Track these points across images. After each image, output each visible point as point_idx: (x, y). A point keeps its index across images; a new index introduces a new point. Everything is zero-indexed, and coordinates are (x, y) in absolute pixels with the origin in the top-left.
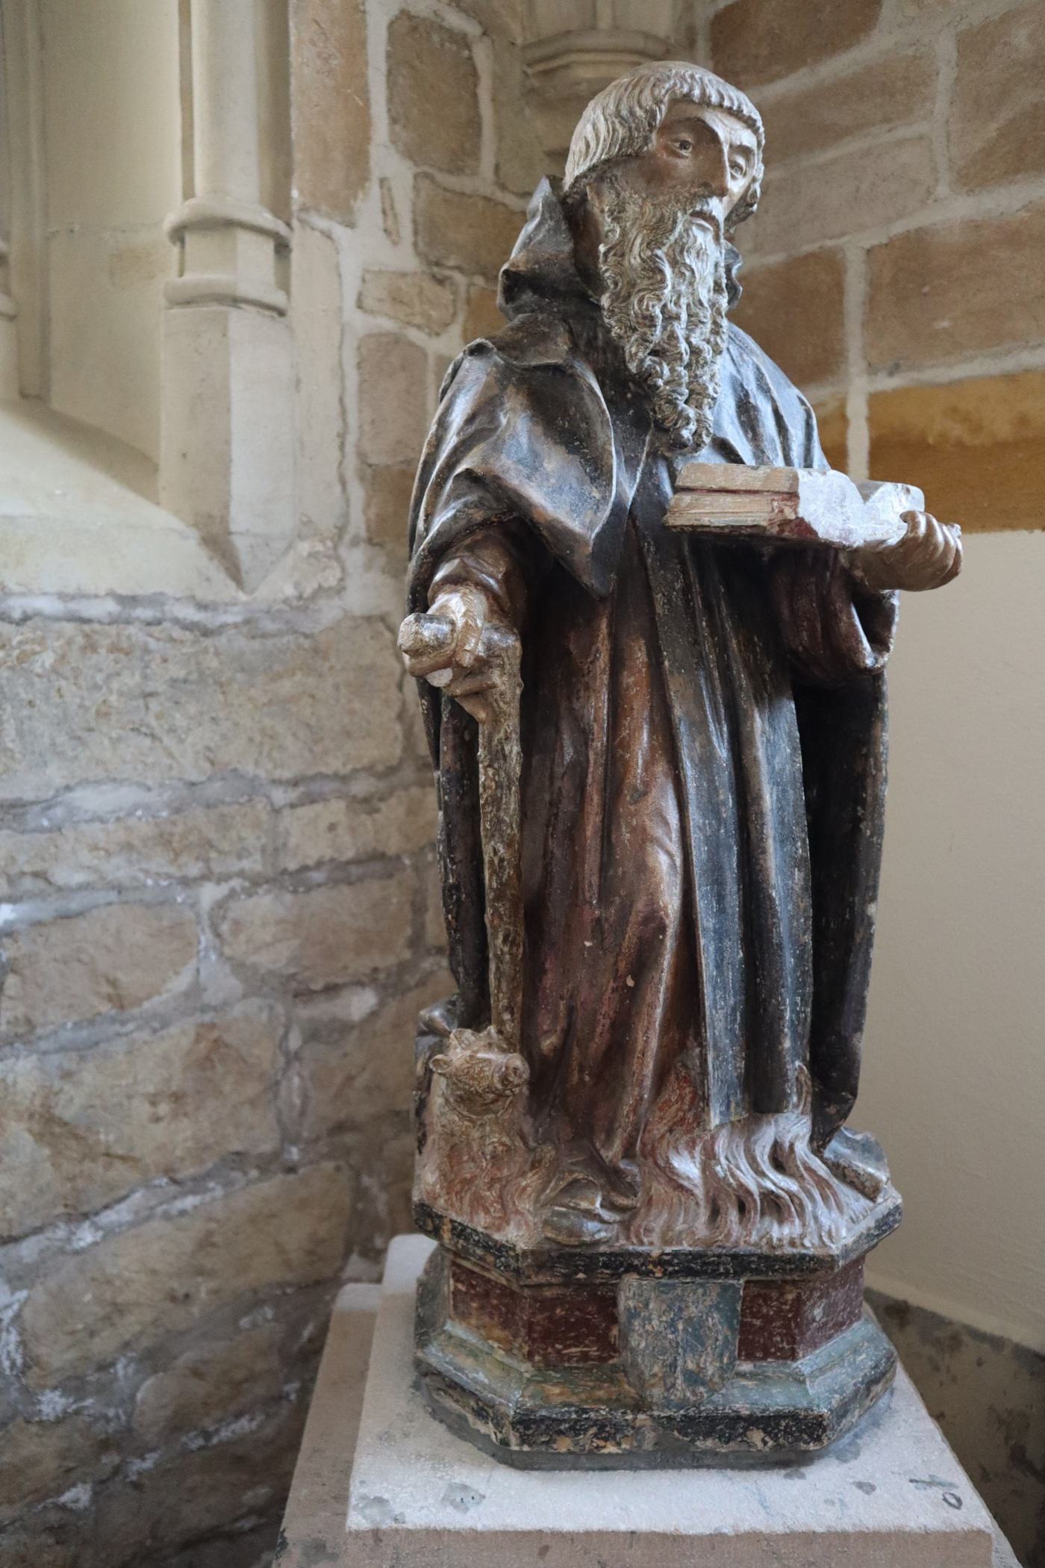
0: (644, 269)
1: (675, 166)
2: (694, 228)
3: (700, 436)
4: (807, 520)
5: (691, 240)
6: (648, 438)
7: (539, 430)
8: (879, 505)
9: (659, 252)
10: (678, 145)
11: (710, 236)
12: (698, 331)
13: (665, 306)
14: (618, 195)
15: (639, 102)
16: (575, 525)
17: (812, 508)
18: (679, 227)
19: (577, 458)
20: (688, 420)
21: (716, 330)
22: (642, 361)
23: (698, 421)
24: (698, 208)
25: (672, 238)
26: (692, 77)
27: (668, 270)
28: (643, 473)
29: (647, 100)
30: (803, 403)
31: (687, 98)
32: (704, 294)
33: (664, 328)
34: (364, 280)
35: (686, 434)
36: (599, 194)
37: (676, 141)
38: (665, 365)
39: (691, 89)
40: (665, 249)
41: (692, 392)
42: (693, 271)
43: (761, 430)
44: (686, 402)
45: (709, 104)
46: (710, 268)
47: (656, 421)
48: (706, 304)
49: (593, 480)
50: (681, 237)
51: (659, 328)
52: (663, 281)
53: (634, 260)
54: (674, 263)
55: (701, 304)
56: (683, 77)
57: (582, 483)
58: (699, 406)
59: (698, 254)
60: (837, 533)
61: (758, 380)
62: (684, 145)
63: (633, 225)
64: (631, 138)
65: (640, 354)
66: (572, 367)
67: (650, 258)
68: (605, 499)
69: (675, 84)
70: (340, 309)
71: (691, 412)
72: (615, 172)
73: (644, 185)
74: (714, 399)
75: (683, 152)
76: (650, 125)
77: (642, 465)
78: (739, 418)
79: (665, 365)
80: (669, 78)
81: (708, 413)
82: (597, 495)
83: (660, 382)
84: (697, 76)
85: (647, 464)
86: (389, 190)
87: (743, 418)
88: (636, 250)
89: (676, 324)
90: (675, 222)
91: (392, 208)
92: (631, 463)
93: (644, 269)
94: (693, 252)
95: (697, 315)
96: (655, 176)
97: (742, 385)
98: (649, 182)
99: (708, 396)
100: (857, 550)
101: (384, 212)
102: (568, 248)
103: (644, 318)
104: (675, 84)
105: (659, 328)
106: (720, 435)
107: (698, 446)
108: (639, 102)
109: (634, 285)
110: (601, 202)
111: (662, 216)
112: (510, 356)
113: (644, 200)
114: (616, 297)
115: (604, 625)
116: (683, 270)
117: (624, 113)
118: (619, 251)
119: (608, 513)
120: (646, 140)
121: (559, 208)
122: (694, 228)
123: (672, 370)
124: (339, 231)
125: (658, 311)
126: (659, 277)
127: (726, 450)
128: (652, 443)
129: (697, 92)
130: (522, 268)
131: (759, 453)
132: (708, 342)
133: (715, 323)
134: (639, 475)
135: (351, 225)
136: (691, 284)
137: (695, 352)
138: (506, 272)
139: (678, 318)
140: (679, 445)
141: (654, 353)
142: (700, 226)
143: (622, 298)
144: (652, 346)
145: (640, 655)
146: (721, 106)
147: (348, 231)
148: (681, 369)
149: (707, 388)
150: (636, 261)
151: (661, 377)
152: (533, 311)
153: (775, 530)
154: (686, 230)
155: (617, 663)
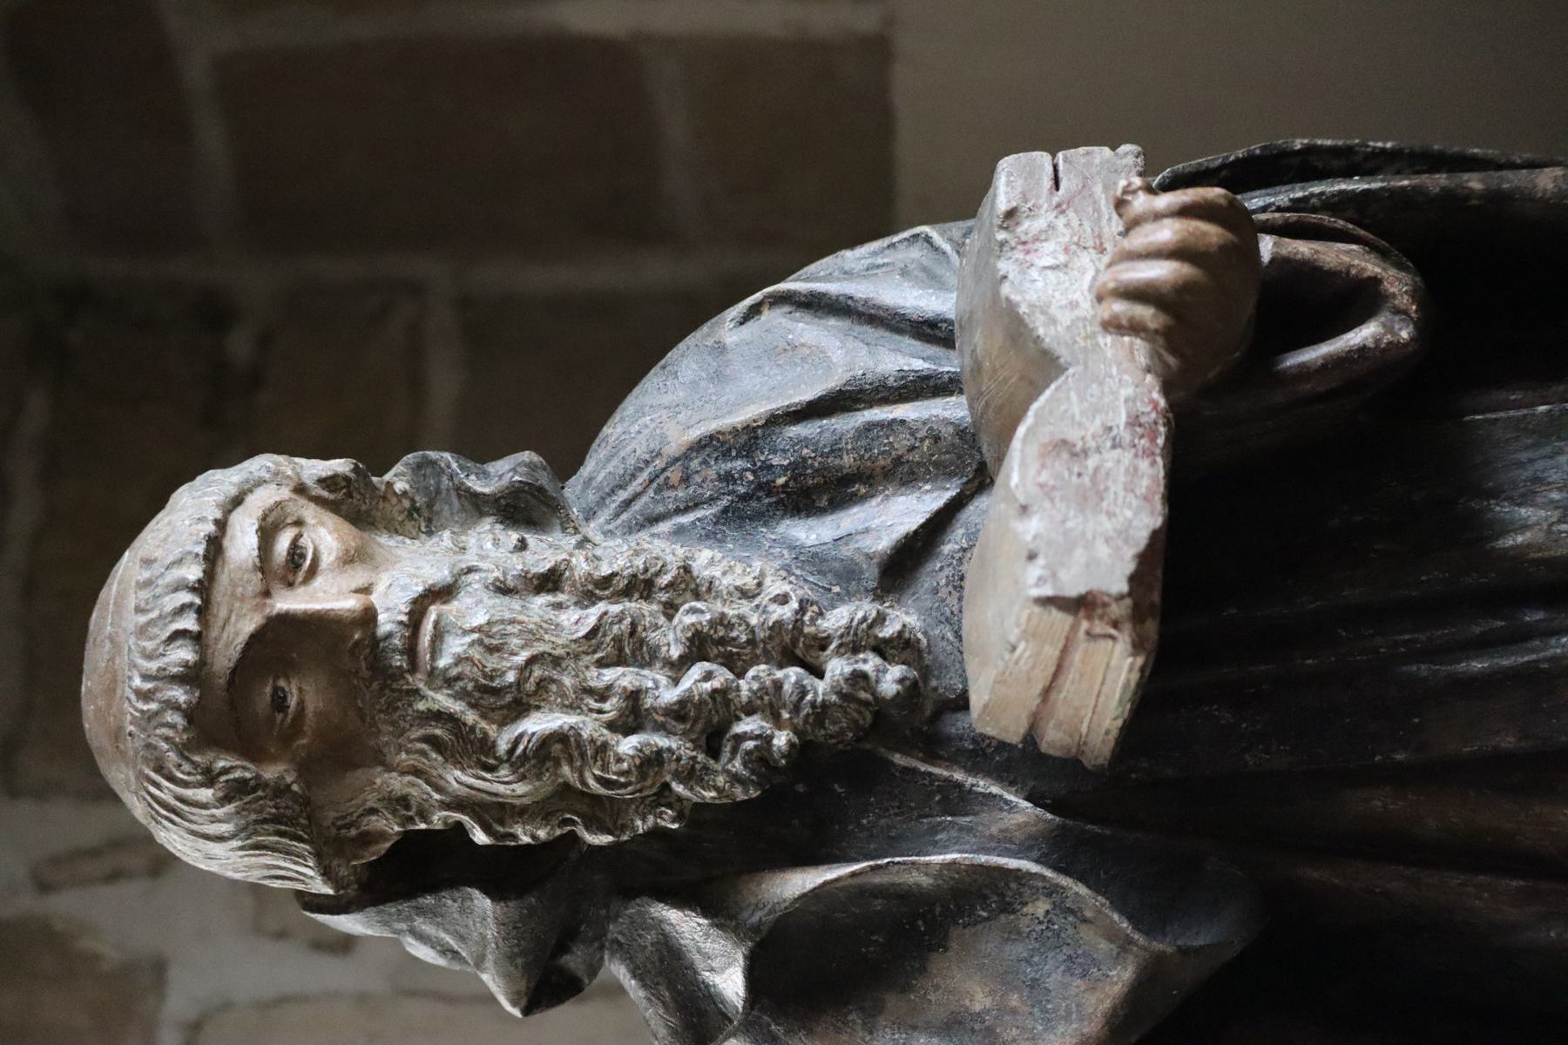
0: (539, 777)
1: (318, 714)
2: (442, 663)
3: (886, 641)
4: (1129, 567)
5: (466, 669)
6: (899, 759)
7: (891, 1000)
8: (1065, 318)
9: (503, 746)
10: (279, 717)
11: (451, 609)
12: (654, 637)
13: (611, 726)
14: (373, 811)
15: (204, 806)
16: (1121, 977)
17: (1103, 551)
18: (443, 700)
19: (954, 932)
20: (858, 678)
21: (640, 586)
22: (735, 778)
23: (856, 650)
24: (398, 661)
25: (471, 717)
26: (145, 696)
27: (538, 724)
28: (973, 770)
29: (205, 794)
30: (755, 311)
31: (191, 714)
32: (576, 620)
33: (659, 728)
34: (281, 935)
35: (891, 679)
36: (367, 839)
37: (271, 720)
38: (740, 728)
39: (176, 707)
40: (492, 730)
41: (789, 657)
42: (532, 661)
43: (848, 460)
44: (819, 673)
45: (201, 664)
46: (509, 607)
47: (859, 740)
48: (593, 614)
49: (1007, 908)
50: (462, 695)
51: (662, 741)
52: (559, 737)
53: (507, 786)
54: (520, 707)
55: (594, 632)
56: (151, 717)
57: (1014, 934)
58: (822, 643)
59: (492, 650)
60: (1144, 464)
61: (726, 455)
62: (279, 702)
63: (438, 789)
64: (276, 820)
65: (721, 780)
66: (756, 929)
67: (515, 767)
68: (1052, 891)
69: (167, 739)
70: (362, 999)
71: (837, 667)
72: (327, 823)
73: (359, 773)
74: (802, 610)
75: (293, 702)
76: (254, 790)
77: (958, 776)
78: (822, 512)
79: (740, 728)
80: (148, 746)
81: (836, 619)
82: (1041, 907)
83: (781, 740)
84: (137, 682)
85: (952, 761)
86: (55, 861)
87: (824, 503)
88: (501, 789)
89: (648, 702)
90: (439, 716)
91: (94, 853)
92: (958, 801)
93: (539, 777)
94: (492, 662)
95: (618, 640)
96: (342, 751)
97: (744, 498)
98: (355, 766)
99: (798, 623)
100: (1167, 388)
101: (114, 877)
102: (482, 903)
103: (643, 776)
104: (167, 739)
105: (662, 741)
106: (871, 574)
107: (899, 648)
108: (204, 806)
109: (567, 786)
110: (382, 836)
111: (428, 739)
112: (720, 1030)
113: (389, 768)
114: (594, 824)
115: (1313, 874)
116: (530, 686)
117: (225, 828)
118: (492, 812)
119: (1082, 890)
120: (280, 790)
121: (391, 908)
122: (442, 663)
123: (750, 710)
124: (179, 1002)
125: (627, 745)
126: (557, 748)
127: (904, 564)
128: (906, 748)
129: (179, 694)
130: (522, 986)
131: (900, 473)
132: (670, 609)
133: (627, 592)
134: (984, 785)
135: (159, 968)
136: (556, 661)
137: (700, 646)
138: (527, 1012)
139: (634, 696)
140: (911, 691)
141: (714, 753)
142: (435, 651)
143: (599, 811)
144: (701, 757)
145: (1379, 803)
146: (197, 638)
147: (174, 974)
148: (746, 686)
149: (779, 624)
150: (521, 788)
151: (768, 740)
152: (602, 948)
153: (1151, 627)
154: (449, 682)
155: (1391, 846)
